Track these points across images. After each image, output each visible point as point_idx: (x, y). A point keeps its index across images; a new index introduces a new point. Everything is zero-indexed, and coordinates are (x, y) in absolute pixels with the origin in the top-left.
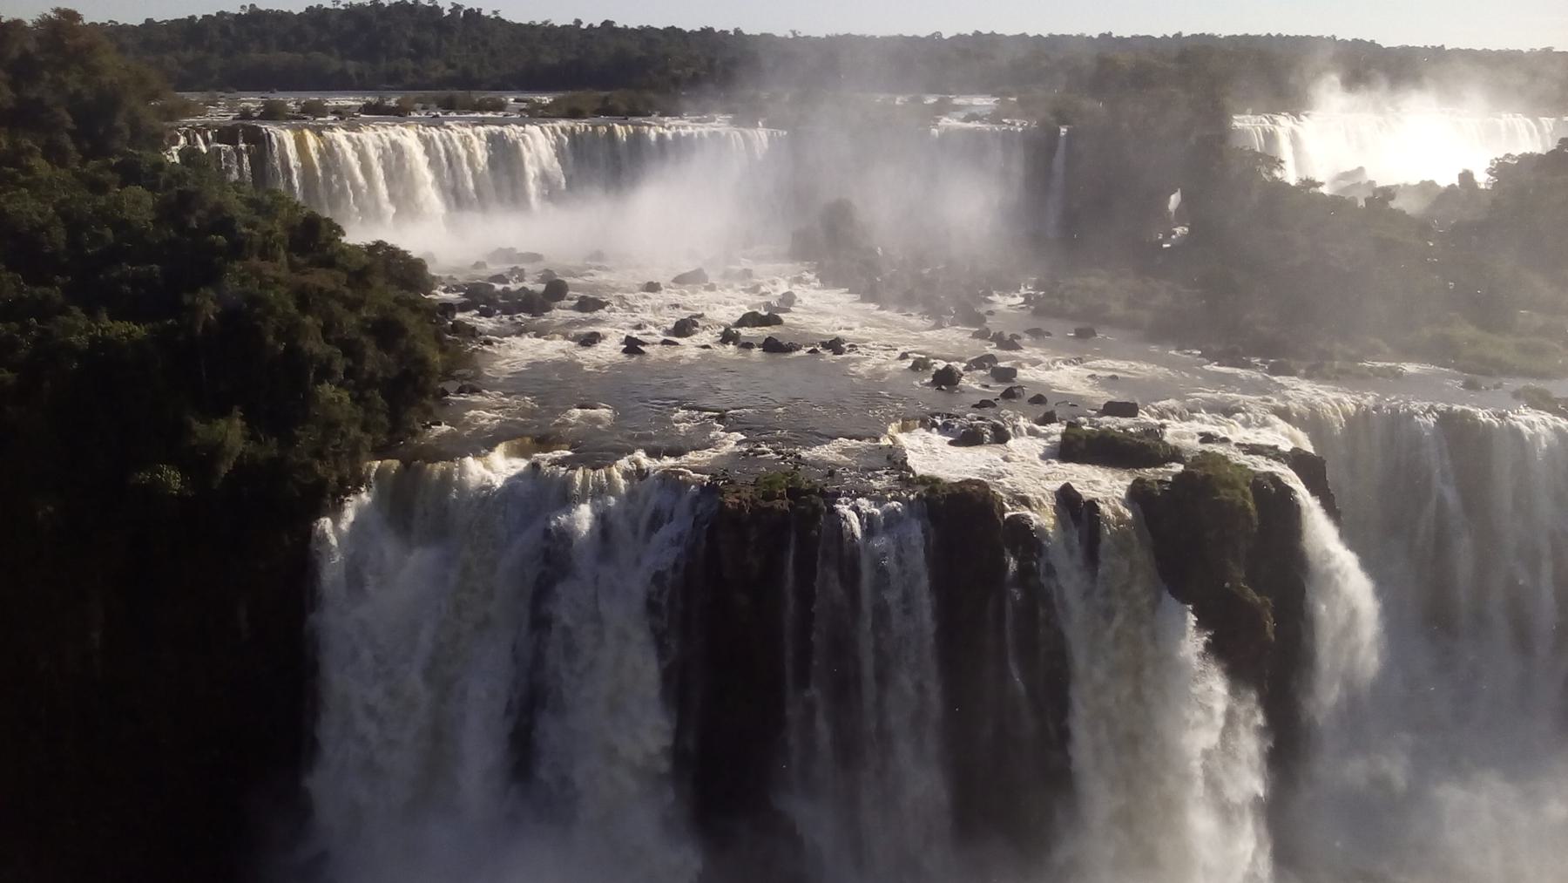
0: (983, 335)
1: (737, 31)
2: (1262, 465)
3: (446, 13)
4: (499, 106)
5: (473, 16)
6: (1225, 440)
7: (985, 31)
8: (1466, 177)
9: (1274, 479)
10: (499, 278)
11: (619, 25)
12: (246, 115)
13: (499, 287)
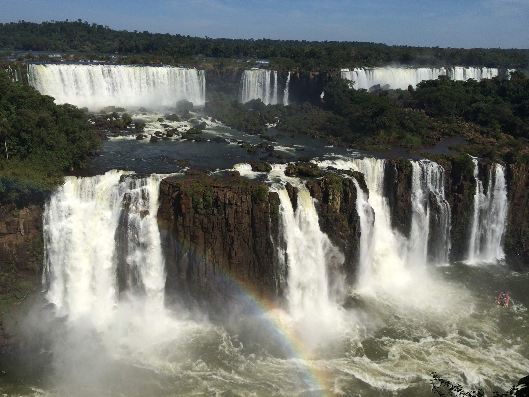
0: (264, 137)
2: (347, 176)
4: (109, 59)
5: (100, 27)
6: (336, 169)
7: (267, 39)
8: (410, 87)
10: (110, 116)
11: (150, 33)
12: (20, 59)
13: (109, 119)
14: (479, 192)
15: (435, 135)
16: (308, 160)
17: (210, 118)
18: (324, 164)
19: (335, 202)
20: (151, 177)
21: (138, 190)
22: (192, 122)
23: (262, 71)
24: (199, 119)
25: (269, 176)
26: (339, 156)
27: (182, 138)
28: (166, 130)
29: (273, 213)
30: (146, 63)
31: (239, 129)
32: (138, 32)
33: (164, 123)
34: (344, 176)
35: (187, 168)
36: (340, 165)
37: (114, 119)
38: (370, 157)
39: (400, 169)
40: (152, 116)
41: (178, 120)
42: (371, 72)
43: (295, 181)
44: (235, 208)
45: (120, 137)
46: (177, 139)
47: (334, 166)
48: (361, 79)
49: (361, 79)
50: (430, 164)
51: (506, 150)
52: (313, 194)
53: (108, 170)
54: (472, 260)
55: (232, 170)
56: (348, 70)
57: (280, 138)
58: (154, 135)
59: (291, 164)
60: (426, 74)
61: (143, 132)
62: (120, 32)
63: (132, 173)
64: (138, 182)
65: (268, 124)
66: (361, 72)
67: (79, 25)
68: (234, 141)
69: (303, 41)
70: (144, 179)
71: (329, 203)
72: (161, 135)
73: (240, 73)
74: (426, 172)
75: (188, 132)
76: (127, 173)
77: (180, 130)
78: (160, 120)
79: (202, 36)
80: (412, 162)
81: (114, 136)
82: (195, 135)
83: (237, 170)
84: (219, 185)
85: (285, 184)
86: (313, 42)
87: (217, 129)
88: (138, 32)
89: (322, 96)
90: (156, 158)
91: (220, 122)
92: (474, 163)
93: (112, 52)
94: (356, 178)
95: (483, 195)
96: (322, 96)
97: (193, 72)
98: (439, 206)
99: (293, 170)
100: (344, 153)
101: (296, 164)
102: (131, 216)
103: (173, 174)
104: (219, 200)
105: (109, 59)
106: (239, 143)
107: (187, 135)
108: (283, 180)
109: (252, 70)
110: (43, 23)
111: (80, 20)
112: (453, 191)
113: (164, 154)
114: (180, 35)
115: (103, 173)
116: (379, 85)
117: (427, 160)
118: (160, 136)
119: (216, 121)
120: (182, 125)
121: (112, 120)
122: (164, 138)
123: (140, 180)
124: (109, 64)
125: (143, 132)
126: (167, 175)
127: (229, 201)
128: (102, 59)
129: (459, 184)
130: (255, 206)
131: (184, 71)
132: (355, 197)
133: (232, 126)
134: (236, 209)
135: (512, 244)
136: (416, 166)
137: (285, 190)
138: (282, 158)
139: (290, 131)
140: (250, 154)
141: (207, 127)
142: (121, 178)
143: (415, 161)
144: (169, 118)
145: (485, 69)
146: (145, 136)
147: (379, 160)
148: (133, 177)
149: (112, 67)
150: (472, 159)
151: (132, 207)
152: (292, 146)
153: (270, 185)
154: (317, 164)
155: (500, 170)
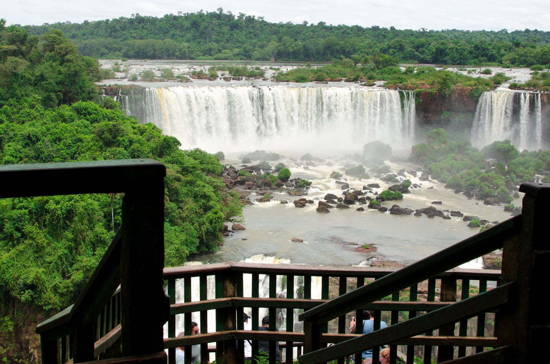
5: (250, 20)
7: (532, 29)
17: (419, 174)
32: (308, 25)
37: (262, 172)
62: (281, 26)
67: (221, 19)
79: (416, 27)
88: (308, 25)
91: (436, 181)
110: (166, 16)
111: (221, 10)
119: (430, 178)
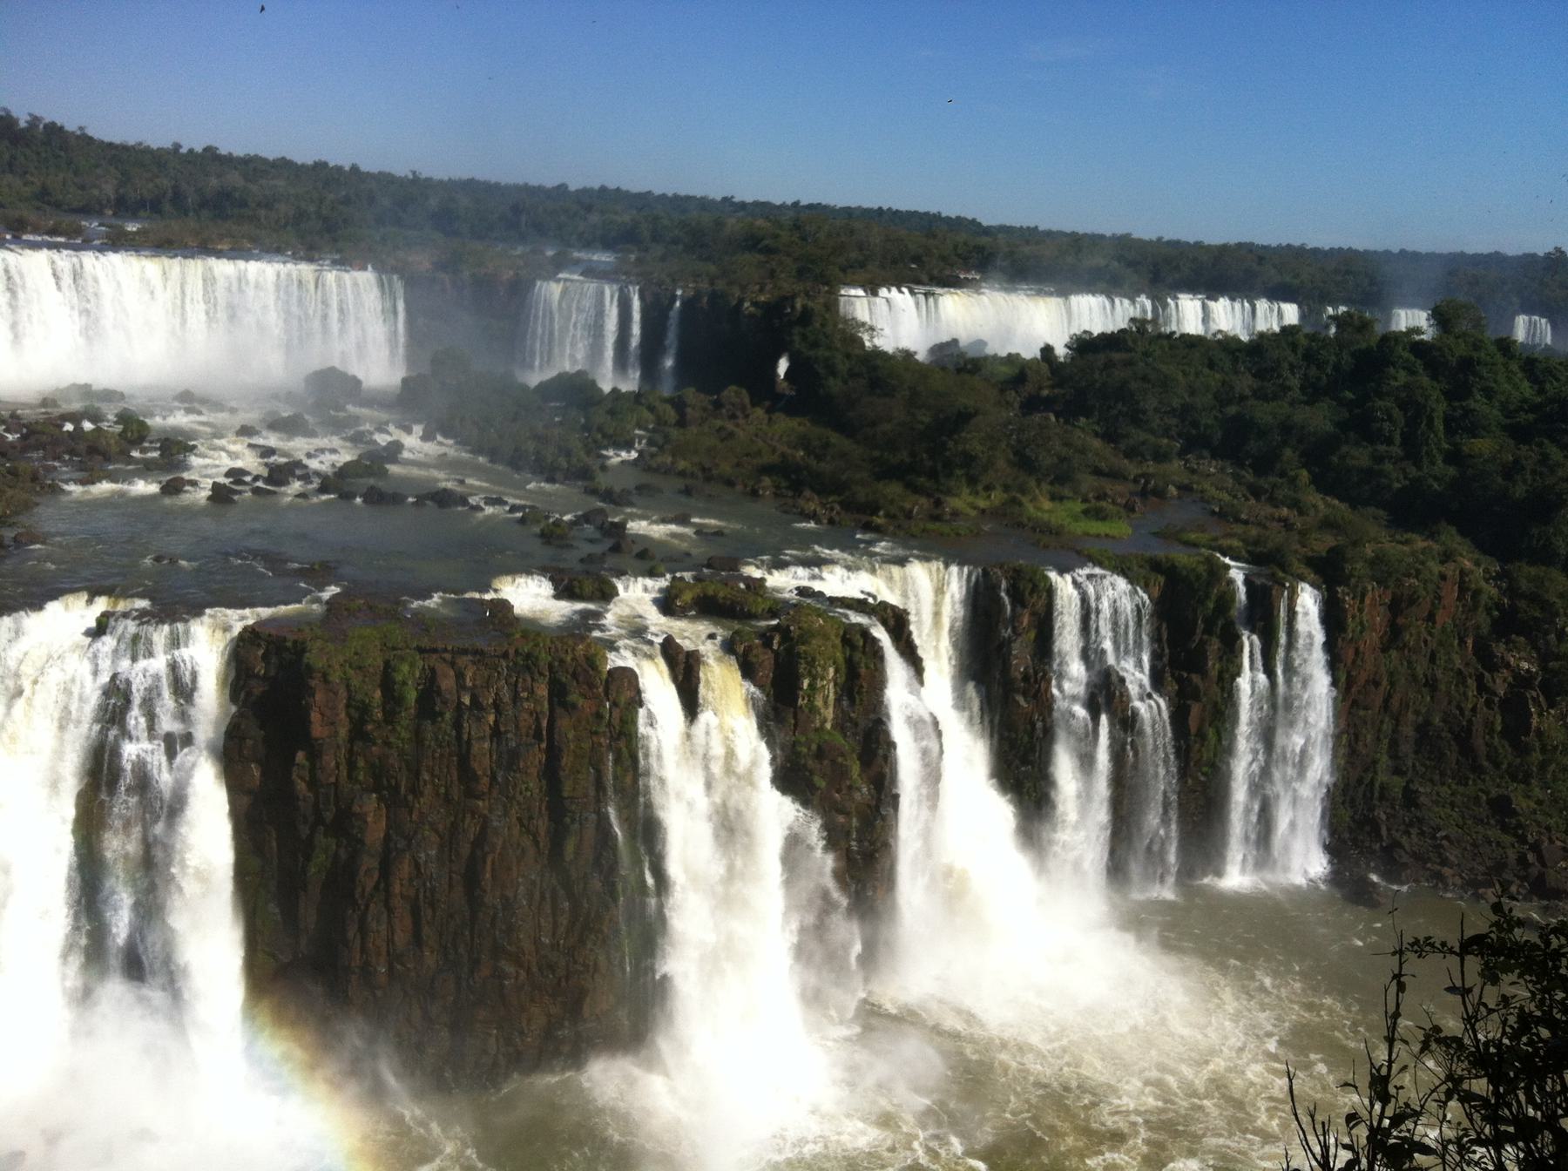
0: (593, 492)
1: (355, 168)
3: (23, 124)
4: (78, 231)
5: (54, 130)
6: (821, 594)
8: (1047, 350)
9: (865, 633)
11: (223, 151)
13: (69, 427)
14: (1252, 668)
15: (1121, 496)
16: (733, 564)
17: (418, 429)
18: (784, 581)
19: (819, 702)
20: (206, 619)
21: (158, 664)
22: (357, 439)
23: (591, 287)
24: (381, 429)
25: (610, 619)
26: (836, 553)
27: (323, 489)
28: (266, 465)
29: (621, 733)
30: (205, 248)
31: (516, 462)
32: (184, 150)
33: (261, 441)
34: (846, 616)
35: (332, 590)
36: (838, 582)
37: (88, 426)
38: (927, 559)
39: (1017, 598)
40: (220, 417)
41: (311, 434)
42: (931, 300)
43: (694, 634)
44: (491, 718)
45: (105, 487)
46: (302, 495)
47: (817, 586)
48: (897, 321)
49: (897, 321)
50: (1106, 582)
51: (1323, 543)
52: (748, 671)
53: (55, 595)
54: (1236, 878)
55: (488, 597)
56: (860, 292)
57: (644, 495)
58: (222, 480)
59: (682, 578)
60: (1095, 314)
61: (187, 468)
63: (142, 604)
64: (160, 635)
65: (611, 453)
66: (901, 299)
68: (498, 501)
69: (725, 199)
70: (180, 626)
71: (800, 701)
72: (248, 479)
73: (520, 290)
74: (1096, 609)
75: (343, 472)
76: (122, 606)
77: (314, 464)
78: (245, 431)
79: (400, 169)
80: (1053, 575)
81: (83, 482)
82: (366, 482)
83: (503, 595)
84: (440, 645)
85: (659, 640)
86: (756, 204)
87: (442, 462)
88: (184, 150)
89: (783, 366)
90: (227, 554)
91: (450, 442)
92: (1231, 582)
93: (86, 211)
94: (884, 623)
95: (1262, 678)
96: (783, 366)
97: (366, 279)
98: (1135, 713)
99: (688, 597)
100: (849, 546)
101: (697, 579)
102: (130, 750)
103: (283, 609)
104: (439, 693)
105: (78, 231)
106: (514, 509)
107: (338, 482)
108: (652, 629)
109: (558, 281)
112: (1173, 663)
113: (255, 543)
114: (325, 164)
115: (37, 604)
116: (955, 341)
117: (1097, 571)
118: (245, 483)
120: (322, 451)
121: (78, 428)
122: (257, 491)
123: (166, 628)
124: (76, 248)
125: (187, 468)
126: (265, 612)
127: (474, 699)
128: (53, 232)
129: (1194, 642)
130: (559, 711)
131: (331, 276)
132: (878, 681)
133: (493, 455)
134: (496, 721)
135: (1353, 826)
136: (1064, 587)
137: (661, 661)
138: (652, 558)
139: (682, 474)
140: (548, 543)
141: (406, 455)
142: (99, 621)
143: (1061, 572)
144: (277, 425)
145: (1262, 305)
146: (194, 483)
147: (954, 569)
148: (142, 617)
149: (89, 259)
150: (1228, 567)
151: (136, 719)
152: (683, 520)
153: (611, 645)
154: (763, 580)
155: (1308, 601)
